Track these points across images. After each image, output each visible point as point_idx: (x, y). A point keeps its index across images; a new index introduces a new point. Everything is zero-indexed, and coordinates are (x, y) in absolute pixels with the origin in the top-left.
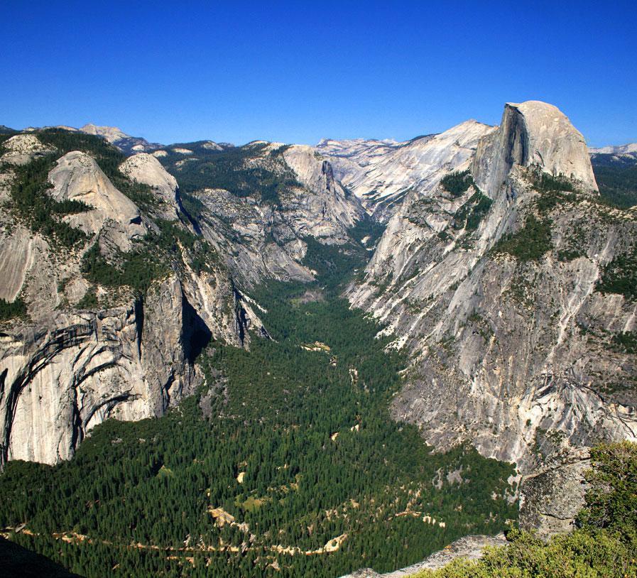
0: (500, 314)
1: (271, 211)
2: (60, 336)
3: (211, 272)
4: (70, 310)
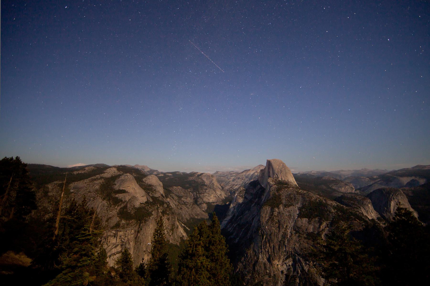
2: (100, 240)
3: (168, 215)
4: (108, 229)
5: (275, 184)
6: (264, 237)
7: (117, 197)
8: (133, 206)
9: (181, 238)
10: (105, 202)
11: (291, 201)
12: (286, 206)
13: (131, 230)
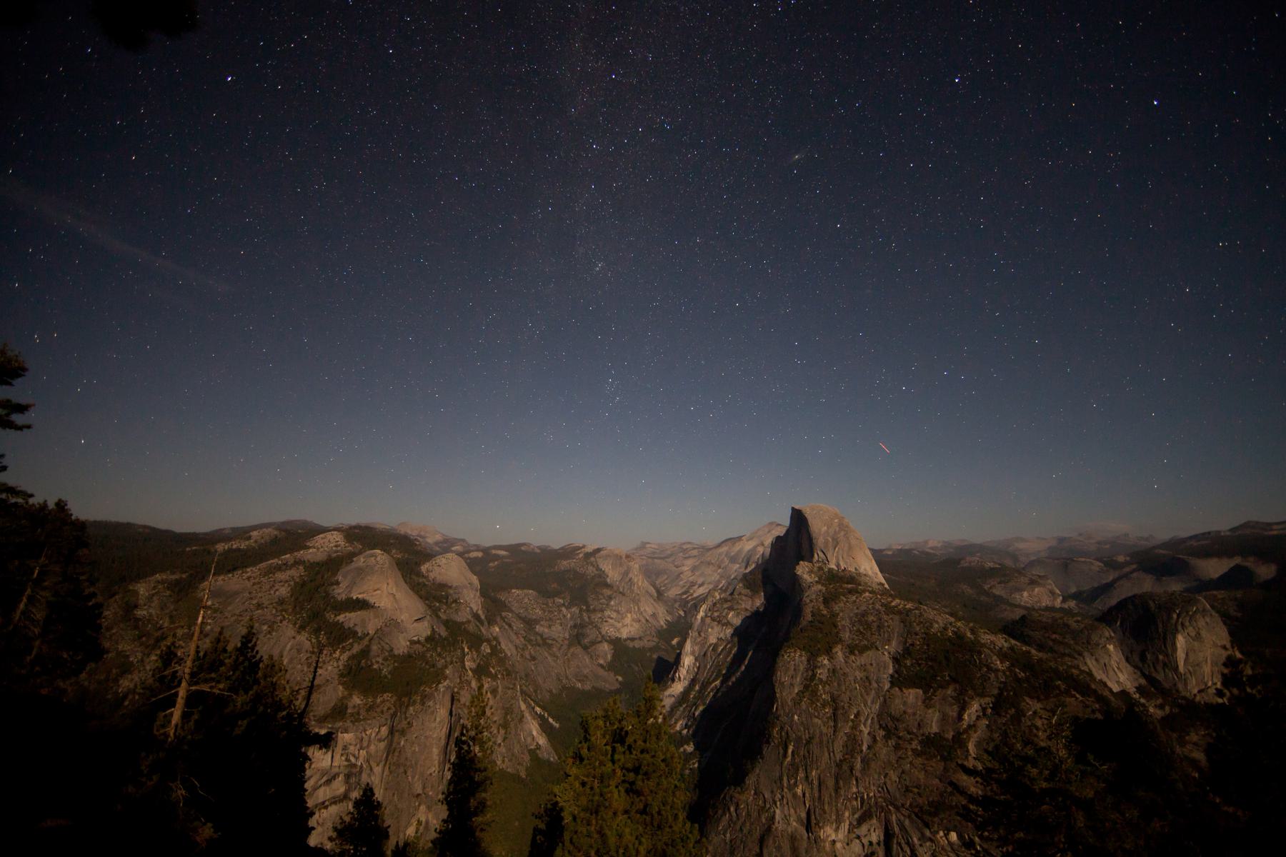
0: (796, 717)
1: (578, 612)
3: (494, 677)
5: (817, 582)
6: (790, 751)
7: (340, 622)
8: (389, 649)
9: (530, 751)
10: (303, 637)
11: (869, 634)
12: (852, 650)
13: (378, 726)
